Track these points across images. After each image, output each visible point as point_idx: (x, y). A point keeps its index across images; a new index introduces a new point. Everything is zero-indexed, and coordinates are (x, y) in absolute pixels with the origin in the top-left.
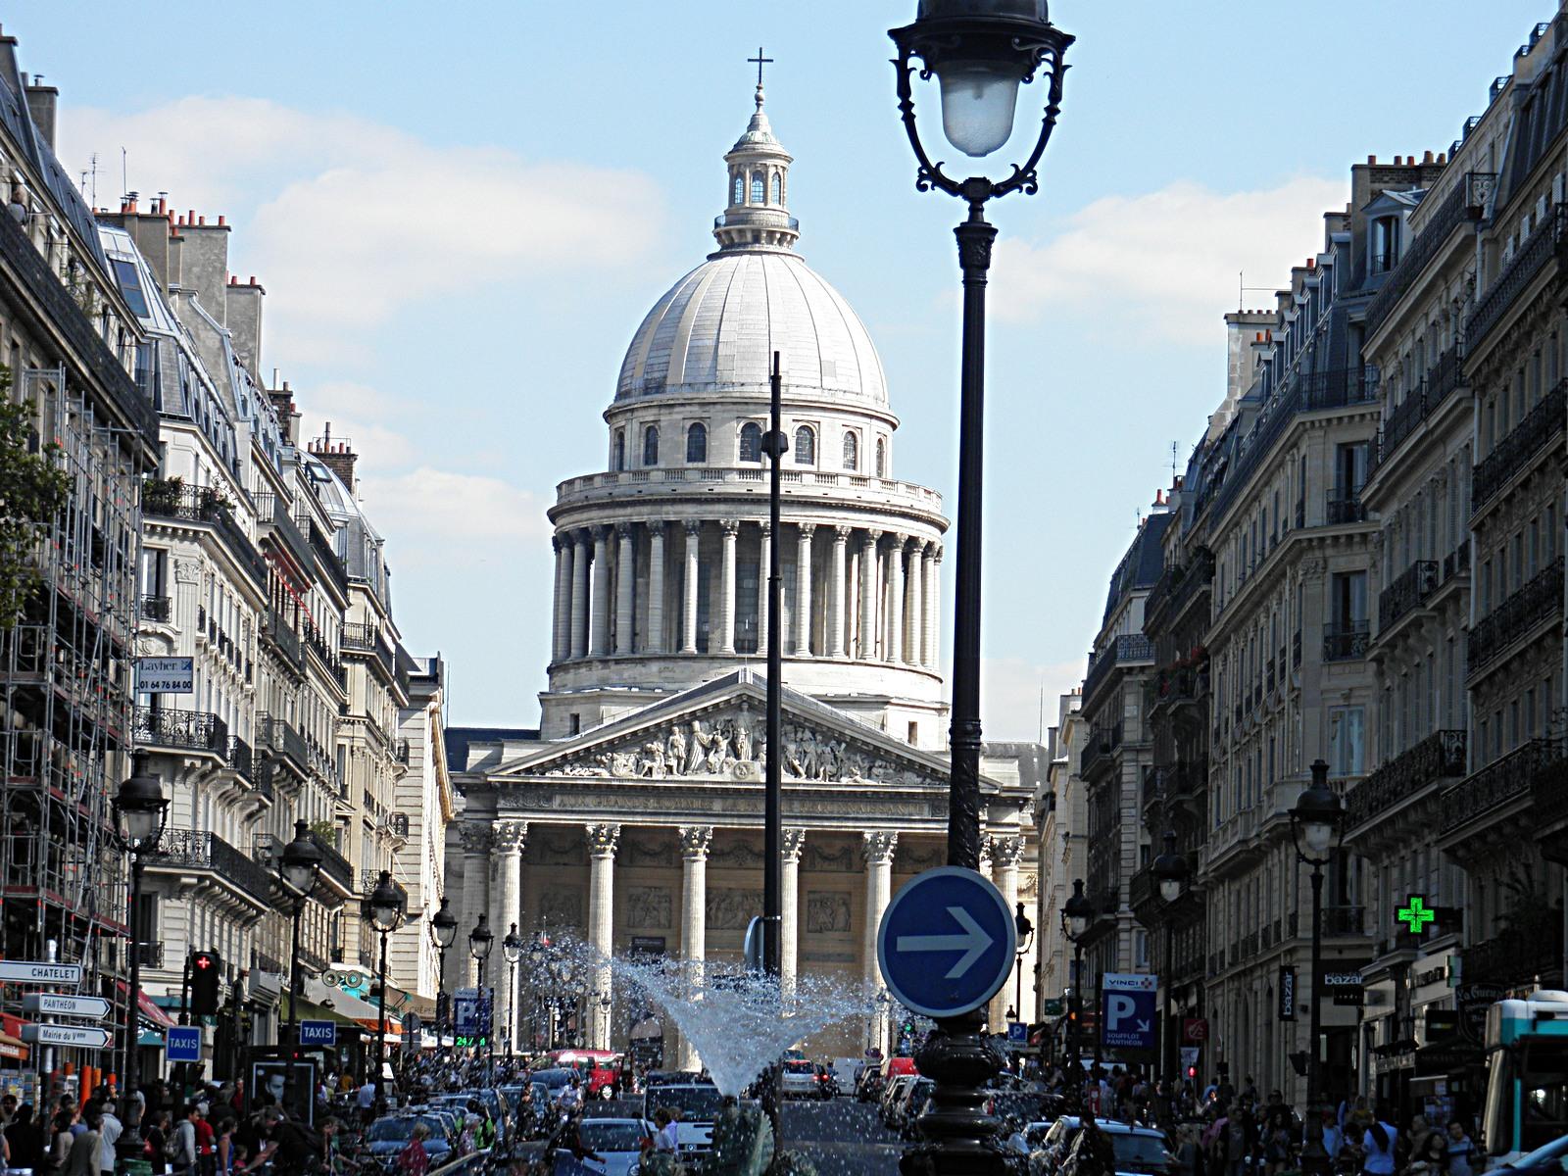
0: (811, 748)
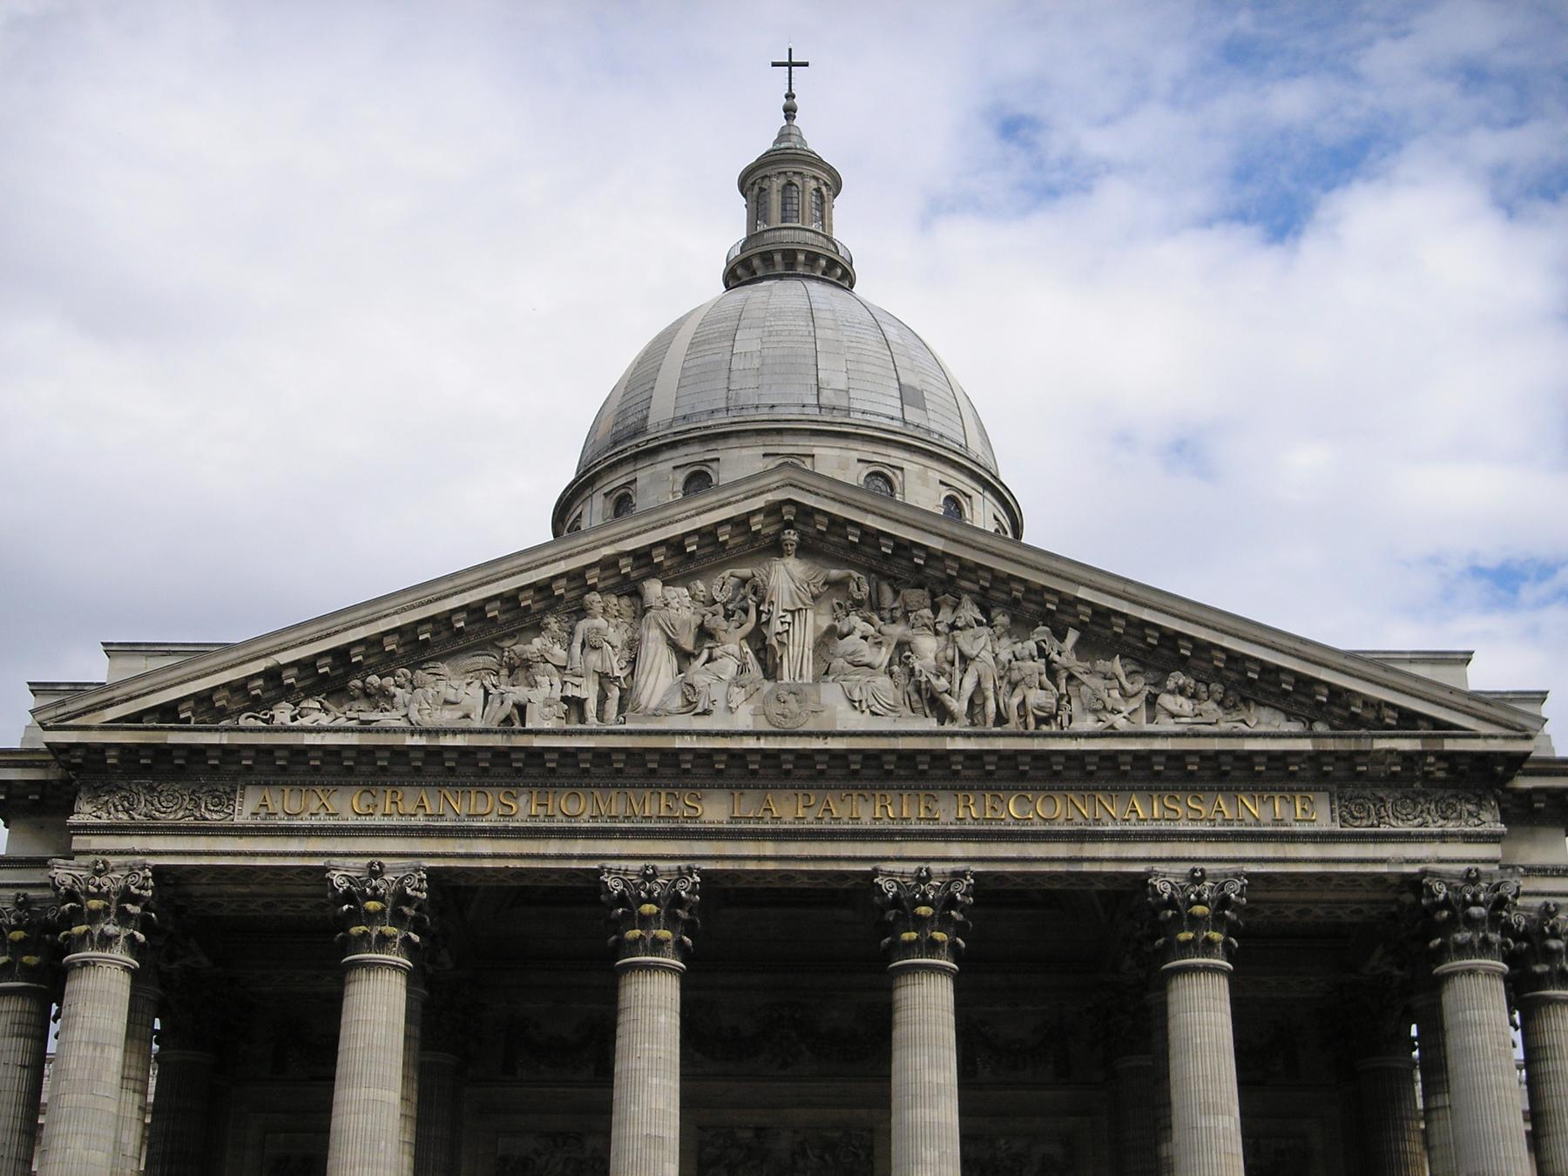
0: (978, 642)
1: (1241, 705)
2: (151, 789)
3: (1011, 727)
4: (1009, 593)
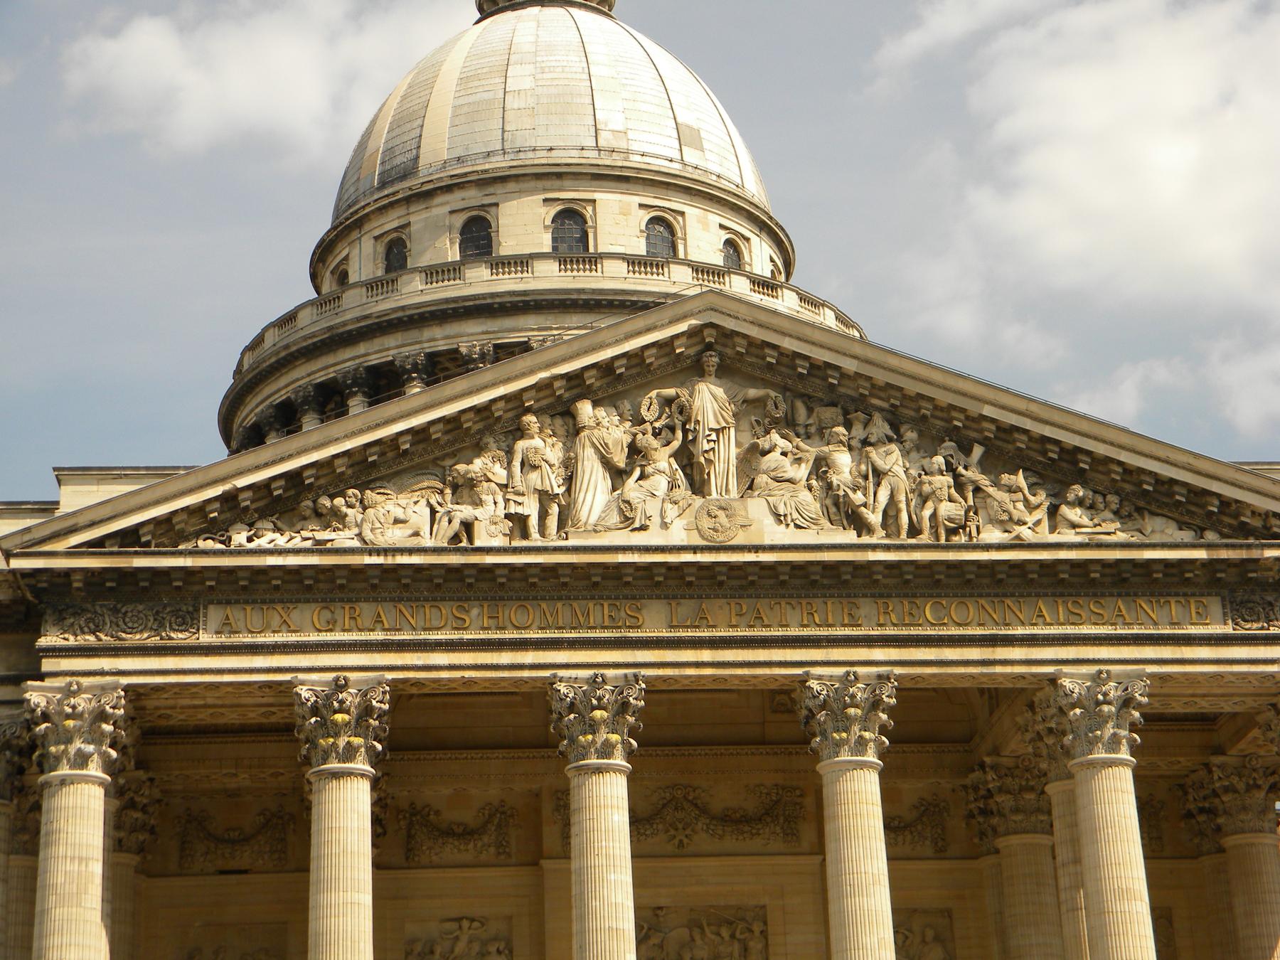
0: (891, 459)
1: (1136, 515)
2: (115, 611)
3: (925, 538)
4: (918, 410)
